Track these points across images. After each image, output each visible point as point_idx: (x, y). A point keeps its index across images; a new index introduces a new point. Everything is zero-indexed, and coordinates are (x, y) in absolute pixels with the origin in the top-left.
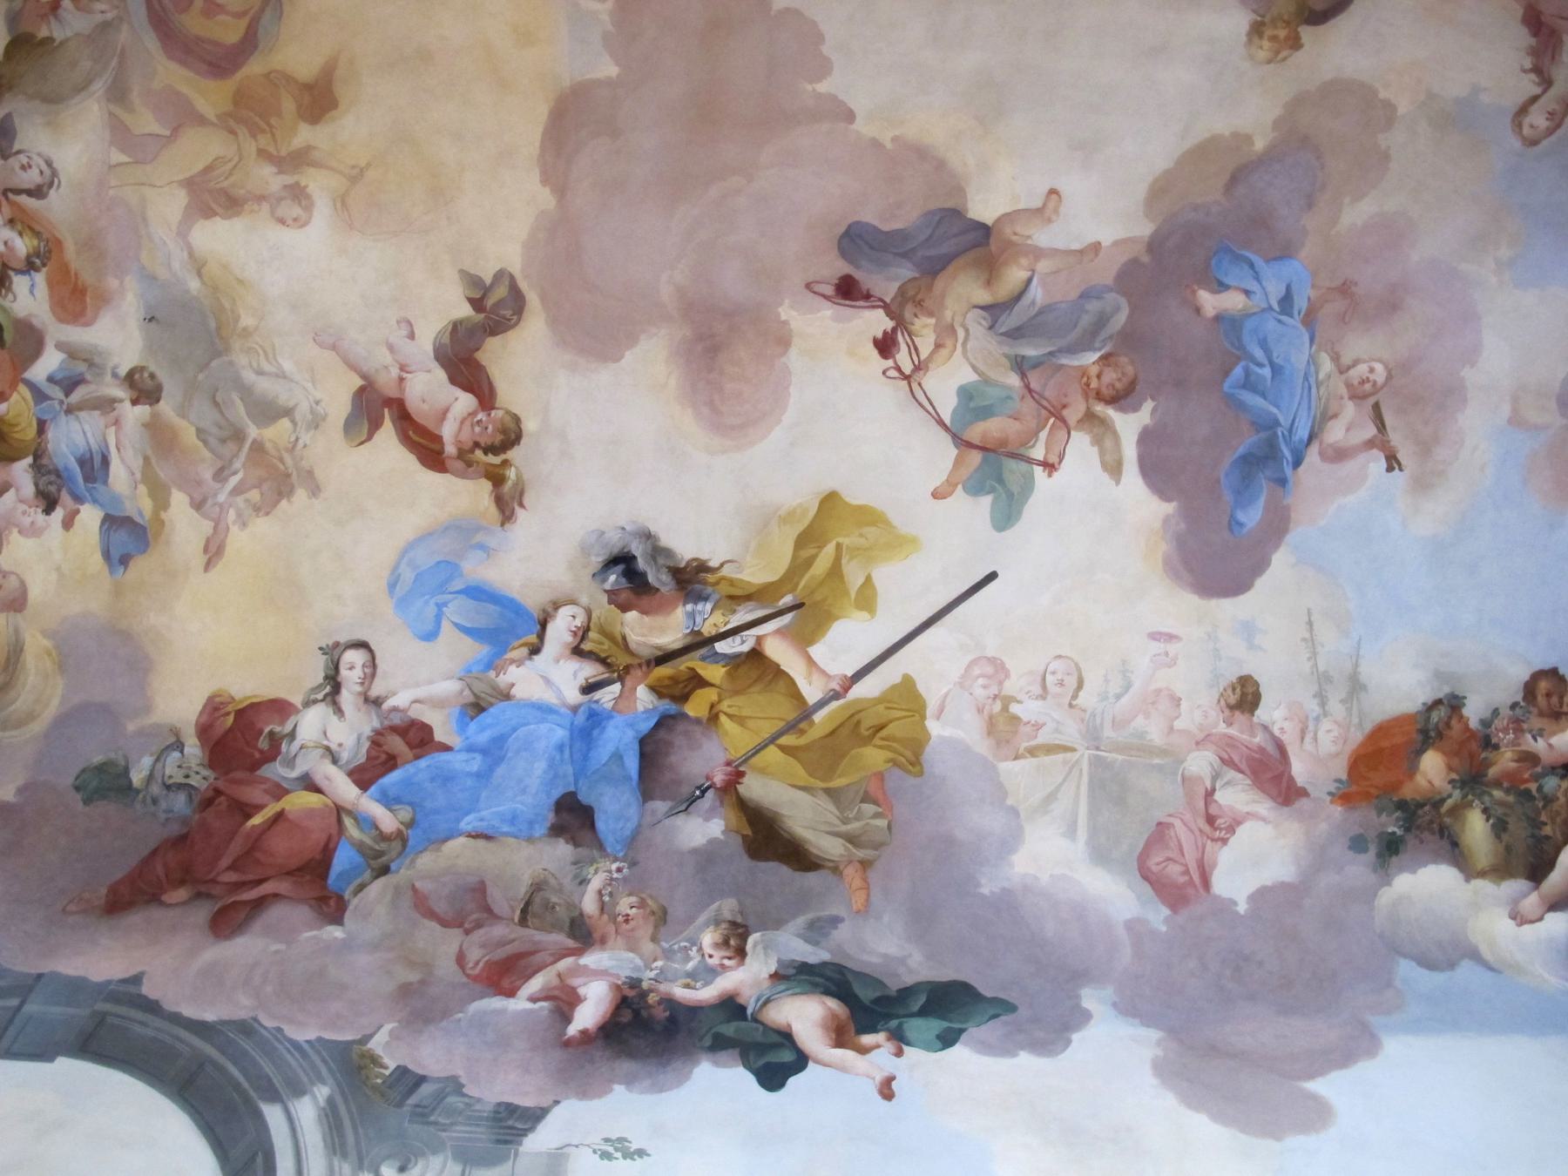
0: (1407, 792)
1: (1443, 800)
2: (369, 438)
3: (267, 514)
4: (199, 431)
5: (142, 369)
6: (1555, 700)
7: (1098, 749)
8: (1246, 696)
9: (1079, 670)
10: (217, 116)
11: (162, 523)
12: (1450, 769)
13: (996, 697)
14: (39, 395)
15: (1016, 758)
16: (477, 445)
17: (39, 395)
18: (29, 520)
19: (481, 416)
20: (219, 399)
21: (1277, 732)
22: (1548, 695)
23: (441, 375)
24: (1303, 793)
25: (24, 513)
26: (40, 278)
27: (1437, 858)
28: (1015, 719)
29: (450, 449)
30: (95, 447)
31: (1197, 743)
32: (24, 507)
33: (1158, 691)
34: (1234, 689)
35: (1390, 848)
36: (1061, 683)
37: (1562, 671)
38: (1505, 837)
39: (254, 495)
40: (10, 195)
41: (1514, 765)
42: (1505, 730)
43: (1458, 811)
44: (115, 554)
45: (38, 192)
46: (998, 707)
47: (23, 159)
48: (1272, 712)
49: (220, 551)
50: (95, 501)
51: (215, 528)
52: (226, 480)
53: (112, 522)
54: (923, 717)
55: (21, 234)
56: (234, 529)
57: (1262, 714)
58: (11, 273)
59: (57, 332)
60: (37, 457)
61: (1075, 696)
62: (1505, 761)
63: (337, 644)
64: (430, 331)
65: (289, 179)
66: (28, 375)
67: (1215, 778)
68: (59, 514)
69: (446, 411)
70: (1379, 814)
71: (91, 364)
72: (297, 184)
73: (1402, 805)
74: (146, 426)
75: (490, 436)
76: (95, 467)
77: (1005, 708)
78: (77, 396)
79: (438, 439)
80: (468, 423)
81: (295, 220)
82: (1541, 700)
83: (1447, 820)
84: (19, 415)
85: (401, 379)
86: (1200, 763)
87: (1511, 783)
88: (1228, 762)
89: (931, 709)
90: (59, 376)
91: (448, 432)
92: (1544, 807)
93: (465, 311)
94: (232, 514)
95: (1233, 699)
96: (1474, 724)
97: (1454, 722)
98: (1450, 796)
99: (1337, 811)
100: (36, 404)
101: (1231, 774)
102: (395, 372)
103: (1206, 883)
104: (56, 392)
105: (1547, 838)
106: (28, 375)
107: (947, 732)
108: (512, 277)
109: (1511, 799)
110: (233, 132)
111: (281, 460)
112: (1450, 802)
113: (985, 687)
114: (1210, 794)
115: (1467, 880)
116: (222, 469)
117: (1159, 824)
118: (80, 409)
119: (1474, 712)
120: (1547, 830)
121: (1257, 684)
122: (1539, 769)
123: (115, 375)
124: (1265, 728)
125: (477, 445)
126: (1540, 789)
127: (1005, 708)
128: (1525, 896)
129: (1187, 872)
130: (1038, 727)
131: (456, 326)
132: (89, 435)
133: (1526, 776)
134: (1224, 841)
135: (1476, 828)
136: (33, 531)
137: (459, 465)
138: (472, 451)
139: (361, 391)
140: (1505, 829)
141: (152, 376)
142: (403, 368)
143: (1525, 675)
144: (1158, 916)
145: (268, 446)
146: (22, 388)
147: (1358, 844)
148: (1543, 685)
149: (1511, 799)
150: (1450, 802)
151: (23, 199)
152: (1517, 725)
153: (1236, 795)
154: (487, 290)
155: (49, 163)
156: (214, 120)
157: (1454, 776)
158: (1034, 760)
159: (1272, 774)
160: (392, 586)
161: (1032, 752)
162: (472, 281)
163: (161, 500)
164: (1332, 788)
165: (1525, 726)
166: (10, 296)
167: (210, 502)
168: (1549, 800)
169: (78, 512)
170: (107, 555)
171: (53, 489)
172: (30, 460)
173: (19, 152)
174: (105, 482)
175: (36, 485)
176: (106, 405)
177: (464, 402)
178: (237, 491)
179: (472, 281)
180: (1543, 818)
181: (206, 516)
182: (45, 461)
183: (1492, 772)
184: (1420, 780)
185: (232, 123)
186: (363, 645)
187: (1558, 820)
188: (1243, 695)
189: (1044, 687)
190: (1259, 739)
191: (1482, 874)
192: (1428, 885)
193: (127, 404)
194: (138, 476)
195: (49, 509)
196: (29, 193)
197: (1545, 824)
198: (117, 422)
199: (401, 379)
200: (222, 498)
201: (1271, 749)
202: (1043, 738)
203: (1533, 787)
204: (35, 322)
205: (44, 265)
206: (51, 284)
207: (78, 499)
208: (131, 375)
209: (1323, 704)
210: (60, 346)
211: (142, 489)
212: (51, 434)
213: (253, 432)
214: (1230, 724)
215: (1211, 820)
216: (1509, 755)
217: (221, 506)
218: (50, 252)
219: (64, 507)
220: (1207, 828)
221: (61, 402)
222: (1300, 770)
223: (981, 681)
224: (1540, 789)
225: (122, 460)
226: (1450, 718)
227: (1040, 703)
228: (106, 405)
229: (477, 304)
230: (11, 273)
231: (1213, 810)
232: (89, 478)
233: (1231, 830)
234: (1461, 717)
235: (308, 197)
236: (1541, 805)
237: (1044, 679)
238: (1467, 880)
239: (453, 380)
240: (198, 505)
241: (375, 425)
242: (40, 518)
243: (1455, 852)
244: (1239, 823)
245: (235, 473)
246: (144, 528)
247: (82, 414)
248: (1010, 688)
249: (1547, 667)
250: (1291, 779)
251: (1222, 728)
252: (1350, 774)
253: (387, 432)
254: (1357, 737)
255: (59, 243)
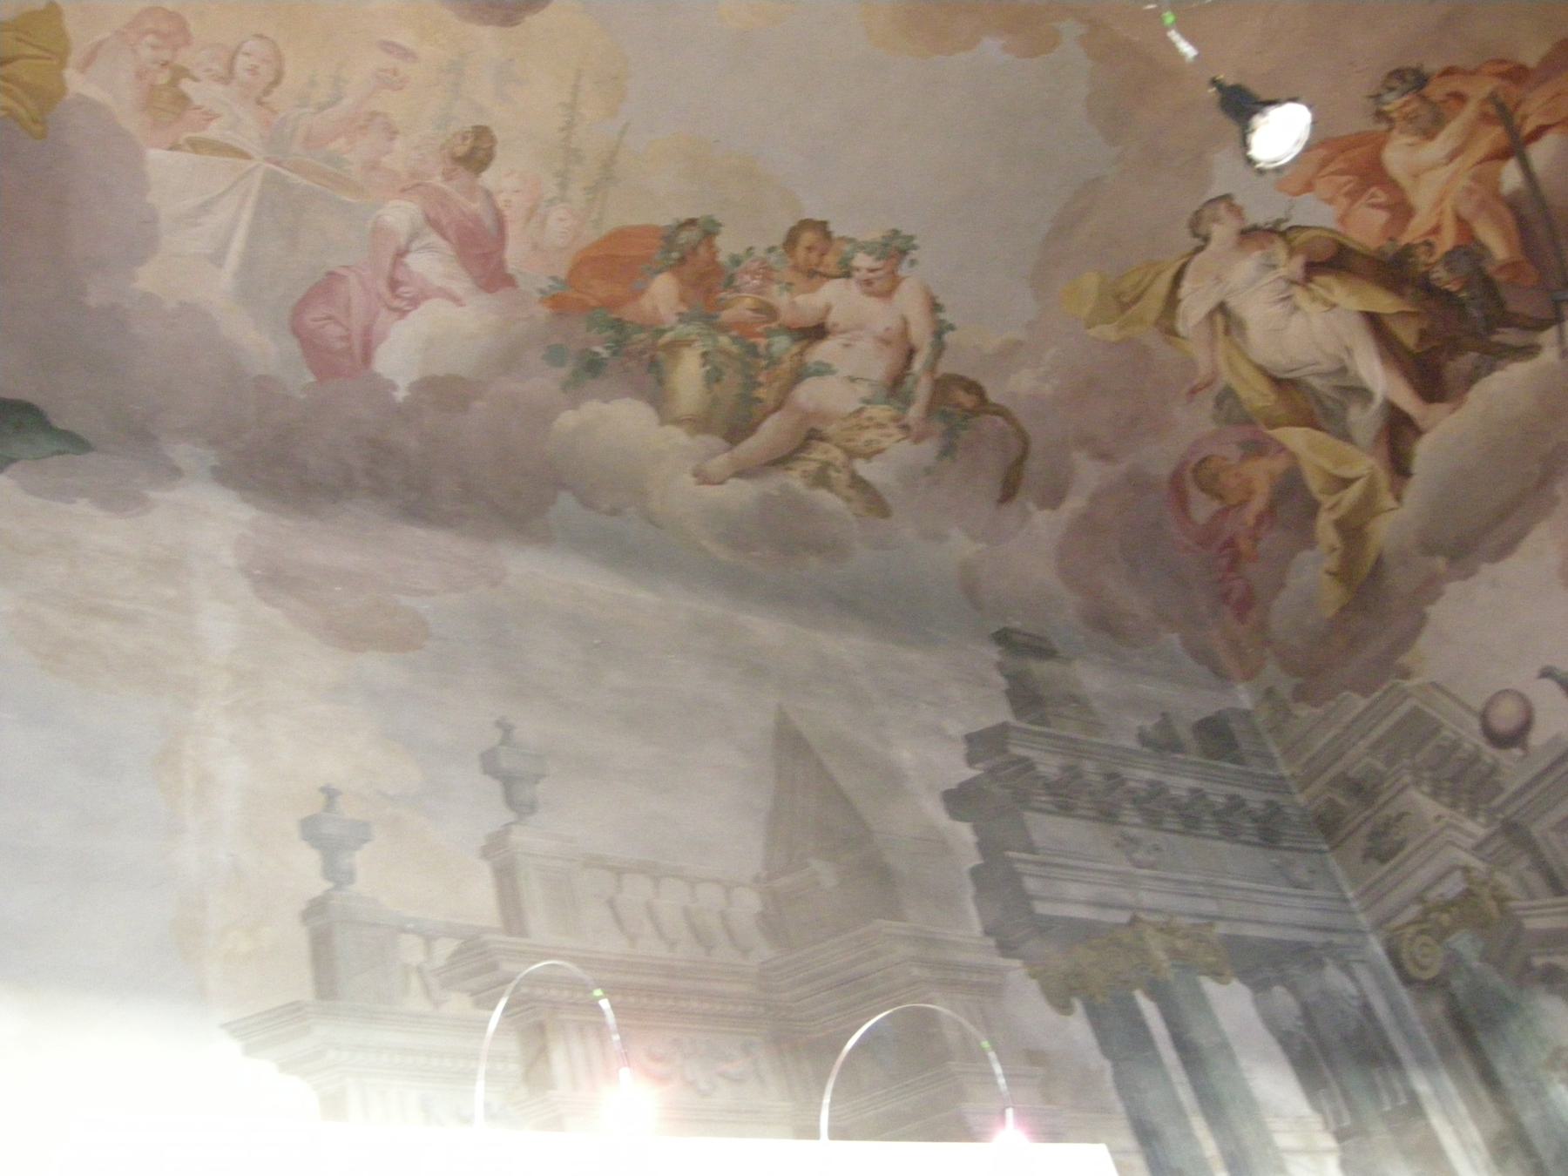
0: (628, 313)
1: (662, 332)
6: (814, 256)
7: (278, 163)
8: (476, 153)
9: (279, 57)
12: (682, 300)
13: (165, 64)
15: (174, 147)
21: (500, 204)
22: (809, 249)
24: (509, 281)
27: (639, 392)
28: (183, 100)
31: (403, 190)
33: (374, 114)
34: (465, 138)
35: (593, 366)
36: (253, 71)
37: (832, 227)
38: (716, 387)
41: (749, 313)
42: (754, 274)
43: (675, 347)
46: (163, 78)
48: (502, 178)
54: (63, 64)
57: (488, 178)
61: (267, 92)
62: (740, 308)
67: (414, 235)
70: (588, 330)
73: (619, 325)
77: (174, 82)
82: (801, 252)
83: (661, 355)
86: (400, 214)
87: (742, 332)
88: (434, 224)
89: (74, 58)
92: (767, 367)
95: (461, 150)
96: (723, 258)
97: (702, 251)
98: (672, 329)
99: (543, 312)
101: (433, 238)
103: (367, 356)
105: (760, 400)
107: (93, 91)
109: (735, 349)
112: (668, 337)
113: (154, 47)
114: (401, 254)
115: (663, 423)
117: (331, 274)
119: (727, 245)
120: (761, 393)
121: (493, 140)
122: (774, 325)
124: (488, 195)
126: (768, 346)
127: (174, 82)
128: (714, 455)
129: (347, 338)
130: (210, 117)
133: (759, 330)
134: (403, 313)
135: (688, 374)
140: (718, 380)
143: (792, 223)
144: (300, 379)
147: (555, 356)
148: (808, 238)
149: (735, 349)
150: (668, 337)
152: (767, 273)
153: (431, 264)
157: (683, 309)
158: (193, 156)
159: (482, 254)
161: (196, 146)
164: (545, 284)
165: (775, 275)
168: (774, 362)
180: (762, 379)
183: (726, 316)
184: (646, 303)
187: (776, 385)
188: (473, 150)
189: (231, 68)
190: (477, 206)
191: (678, 422)
192: (619, 420)
197: (760, 385)
201: (488, 222)
202: (213, 132)
203: (762, 342)
209: (563, 186)
214: (448, 177)
215: (394, 284)
216: (748, 302)
220: (387, 295)
222: (515, 255)
223: (150, 39)
224: (768, 346)
226: (700, 242)
227: (219, 88)
231: (400, 275)
233: (415, 302)
234: (711, 246)
236: (764, 363)
237: (233, 58)
238: (663, 423)
243: (658, 395)
244: (427, 298)
248: (185, 58)
249: (818, 218)
250: (501, 264)
251: (437, 181)
252: (571, 273)
254: (591, 235)
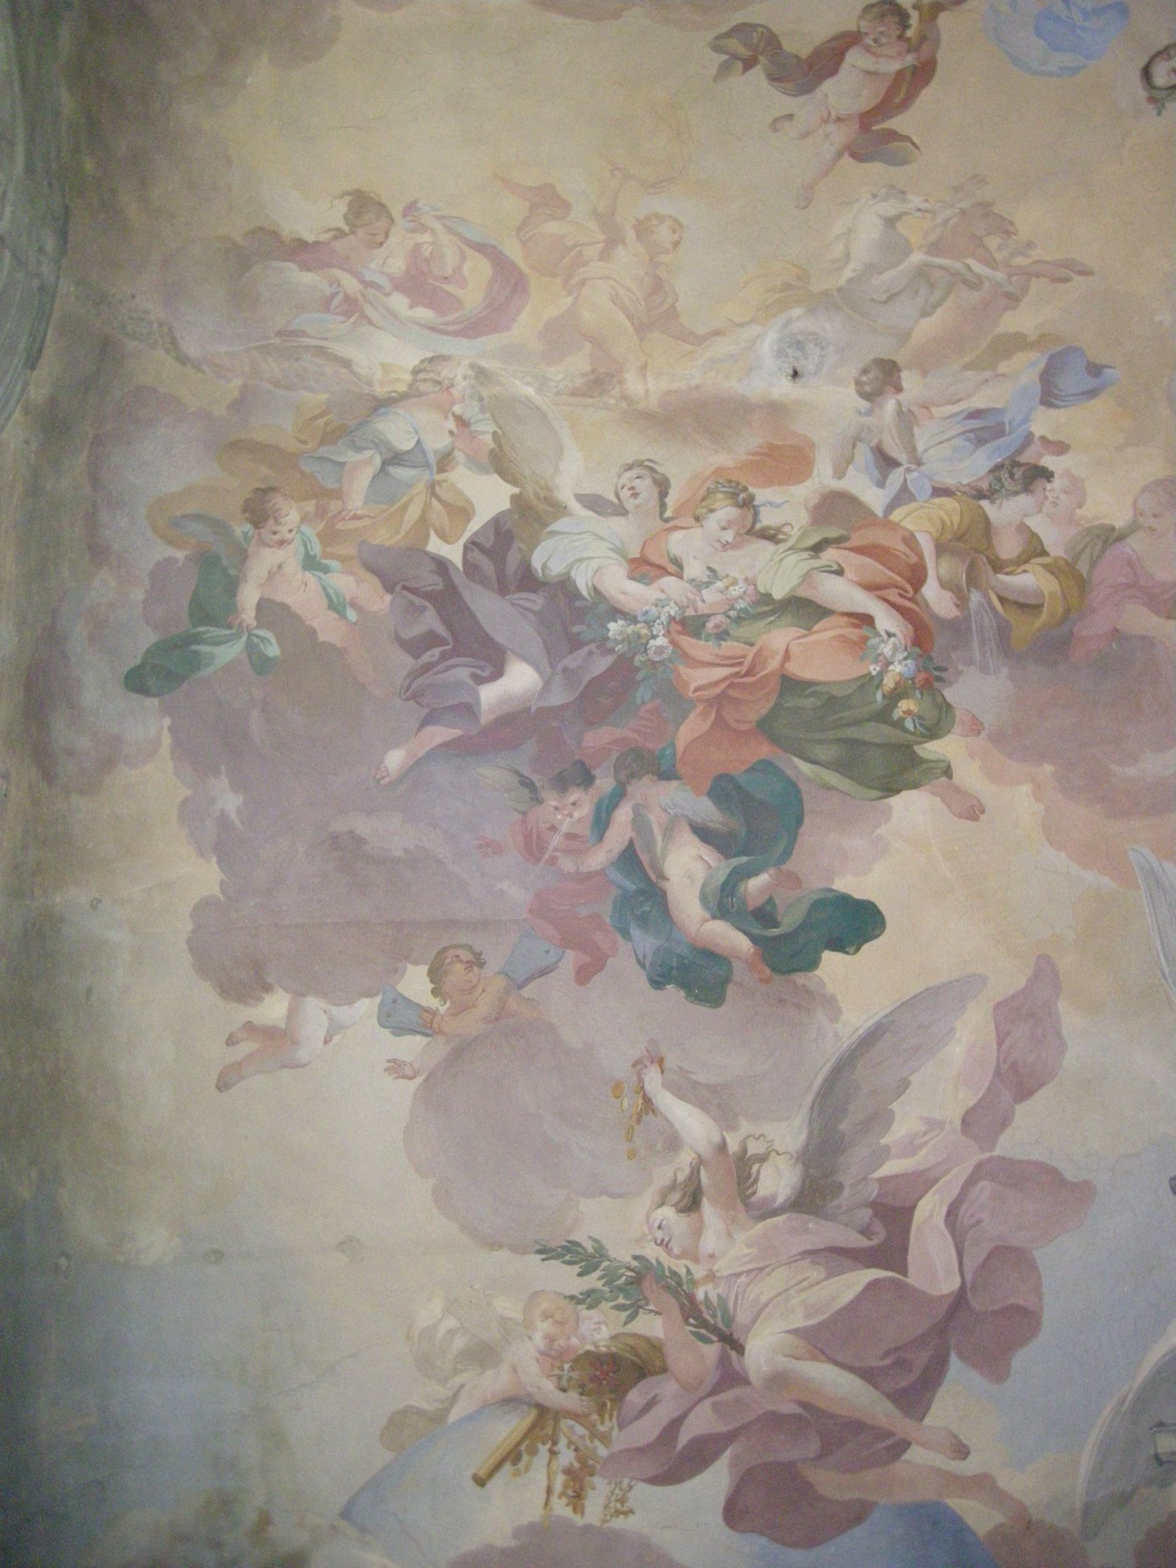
2: (908, 139)
3: (1011, 223)
4: (925, 314)
5: (858, 383)
10: (569, 293)
11: (1042, 336)
14: (904, 495)
16: (901, 37)
17: (904, 495)
18: (1063, 497)
19: (869, 41)
20: (884, 297)
23: (828, 85)
25: (1055, 504)
26: (762, 495)
29: (910, 59)
30: (959, 429)
32: (1047, 503)
39: (993, 242)
40: (668, 514)
44: (1091, 383)
45: (663, 486)
47: (625, 494)
49: (1068, 264)
50: (1026, 420)
51: (1037, 276)
52: (978, 276)
53: (1049, 397)
55: (711, 511)
56: (1035, 254)
58: (758, 526)
59: (823, 477)
60: (980, 495)
63: (1152, 99)
64: (782, 102)
65: (631, 235)
66: (879, 512)
68: (1049, 461)
69: (867, 73)
71: (856, 440)
72: (634, 227)
74: (925, 373)
75: (891, 26)
76: (984, 427)
78: (895, 450)
79: (900, 74)
80: (879, 50)
81: (674, 231)
84: (930, 519)
85: (839, 119)
90: (876, 474)
91: (893, 66)
93: (757, 74)
94: (1020, 261)
100: (912, 498)
102: (830, 128)
104: (896, 478)
106: (879, 512)
108: (718, 38)
110: (583, 283)
111: (946, 222)
116: (965, 282)
118: (914, 449)
123: (870, 412)
125: (901, 37)
131: (773, 79)
132: (950, 434)
136: (1076, 487)
137: (925, 48)
138: (908, 40)
139: (855, 156)
141: (865, 371)
142: (825, 121)
145: (932, 238)
146: (896, 516)
151: (671, 500)
154: (735, 57)
155: (629, 468)
156: (570, 300)
160: (1075, 71)
162: (724, 70)
163: (1014, 344)
166: (786, 529)
167: (1010, 289)
169: (1043, 438)
170: (1092, 393)
171: (1018, 474)
172: (985, 504)
173: (617, 496)
174: (1001, 411)
175: (1016, 493)
176: (906, 420)
177: (855, 58)
178: (989, 261)
179: (724, 70)
181: (1025, 289)
182: (984, 485)
185: (575, 280)
186: (1146, 73)
193: (901, 397)
194: (986, 374)
195: (1048, 475)
196: (663, 494)
198: (925, 407)
199: (839, 119)
200: (1000, 276)
204: (814, 500)
205: (745, 489)
206: (769, 482)
207: (1029, 439)
208: (867, 396)
210: (840, 473)
211: (1003, 367)
212: (949, 481)
213: (917, 257)
217: (1010, 275)
218: (730, 481)
219: (1041, 456)
221: (908, 470)
225: (968, 396)
228: (906, 420)
229: (749, 64)
230: (758, 526)
232: (998, 431)
235: (648, 218)
239: (833, 72)
240: (1013, 300)
241: (893, 135)
242: (1057, 483)
245: (969, 268)
246: (1051, 358)
247: (920, 447)
253: (897, 123)
255: (719, 471)
